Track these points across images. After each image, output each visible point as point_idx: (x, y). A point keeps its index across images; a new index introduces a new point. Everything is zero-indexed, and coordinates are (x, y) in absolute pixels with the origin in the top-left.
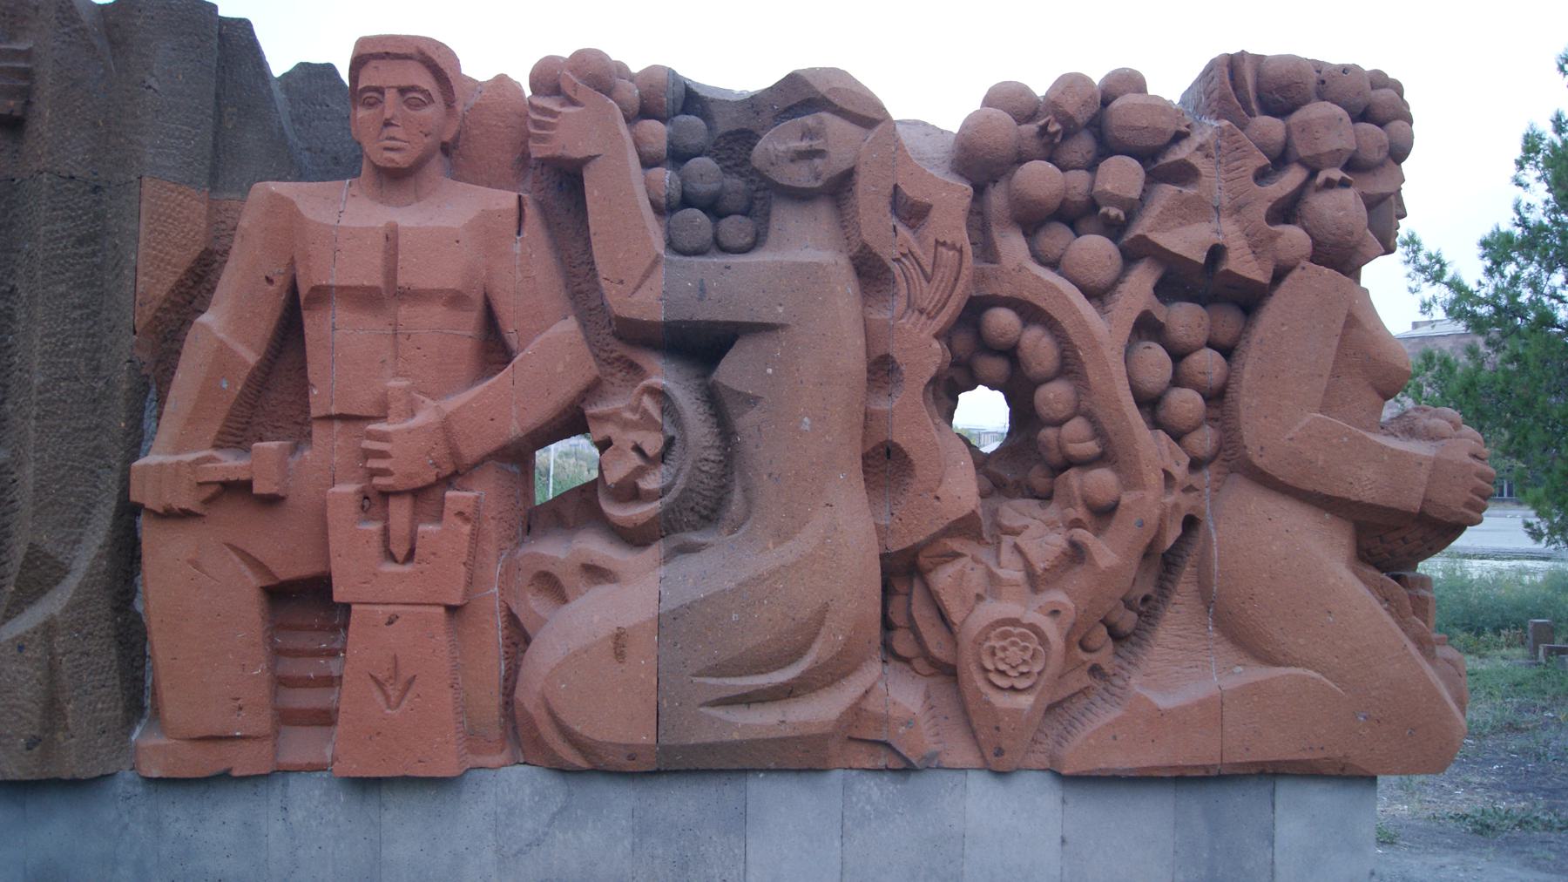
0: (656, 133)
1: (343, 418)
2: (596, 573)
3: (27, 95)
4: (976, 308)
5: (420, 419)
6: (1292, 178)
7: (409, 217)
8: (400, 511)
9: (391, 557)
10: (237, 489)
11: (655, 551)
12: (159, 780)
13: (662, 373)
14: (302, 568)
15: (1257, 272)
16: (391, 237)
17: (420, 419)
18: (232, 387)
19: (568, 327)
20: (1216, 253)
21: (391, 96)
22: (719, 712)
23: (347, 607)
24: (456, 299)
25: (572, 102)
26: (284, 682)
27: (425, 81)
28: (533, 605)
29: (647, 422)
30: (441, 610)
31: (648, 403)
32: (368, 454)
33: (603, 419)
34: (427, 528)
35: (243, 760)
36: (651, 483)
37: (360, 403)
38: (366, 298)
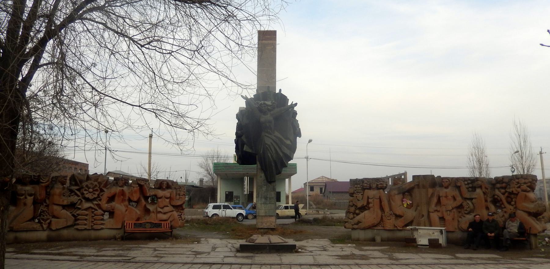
0: (466, 182)
4: (494, 196)
6: (519, 185)
10: (436, 211)
14: (441, 216)
15: (517, 193)
20: (512, 191)
36: (468, 210)
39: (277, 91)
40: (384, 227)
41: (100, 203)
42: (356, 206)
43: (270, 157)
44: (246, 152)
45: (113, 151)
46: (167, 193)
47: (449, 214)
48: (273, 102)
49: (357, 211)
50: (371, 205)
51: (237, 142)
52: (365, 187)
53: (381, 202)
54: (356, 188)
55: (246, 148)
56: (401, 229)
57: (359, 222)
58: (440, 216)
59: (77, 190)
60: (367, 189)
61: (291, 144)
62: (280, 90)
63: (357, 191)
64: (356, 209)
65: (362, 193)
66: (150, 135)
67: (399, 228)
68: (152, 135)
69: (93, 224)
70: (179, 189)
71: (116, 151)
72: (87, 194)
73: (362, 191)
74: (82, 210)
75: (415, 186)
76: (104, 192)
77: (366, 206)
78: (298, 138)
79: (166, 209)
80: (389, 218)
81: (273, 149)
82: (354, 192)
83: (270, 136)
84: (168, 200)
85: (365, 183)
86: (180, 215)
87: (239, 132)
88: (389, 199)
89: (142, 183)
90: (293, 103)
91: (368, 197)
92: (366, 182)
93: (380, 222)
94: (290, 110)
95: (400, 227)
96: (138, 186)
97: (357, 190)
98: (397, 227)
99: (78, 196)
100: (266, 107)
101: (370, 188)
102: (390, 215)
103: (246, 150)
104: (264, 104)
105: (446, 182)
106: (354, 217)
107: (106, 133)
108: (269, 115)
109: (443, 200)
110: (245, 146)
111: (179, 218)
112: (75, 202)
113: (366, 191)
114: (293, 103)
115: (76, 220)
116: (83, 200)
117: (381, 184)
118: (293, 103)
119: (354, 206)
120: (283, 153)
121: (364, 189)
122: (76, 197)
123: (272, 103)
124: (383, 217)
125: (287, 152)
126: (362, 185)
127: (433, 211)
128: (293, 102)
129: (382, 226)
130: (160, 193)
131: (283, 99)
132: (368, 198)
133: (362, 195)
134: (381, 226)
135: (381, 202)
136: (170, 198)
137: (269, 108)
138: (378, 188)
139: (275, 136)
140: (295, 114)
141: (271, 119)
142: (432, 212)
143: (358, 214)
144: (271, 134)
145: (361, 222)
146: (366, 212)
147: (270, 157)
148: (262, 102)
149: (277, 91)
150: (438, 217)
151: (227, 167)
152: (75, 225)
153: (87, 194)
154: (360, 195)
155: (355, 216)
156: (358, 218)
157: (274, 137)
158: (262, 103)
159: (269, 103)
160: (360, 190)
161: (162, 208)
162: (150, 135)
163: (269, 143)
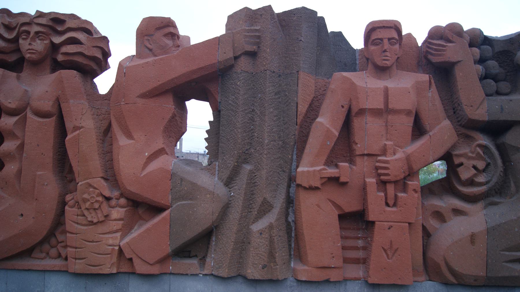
1: (368, 155)
2: (457, 212)
3: (258, 44)
5: (398, 156)
7: (390, 84)
9: (387, 205)
10: (334, 180)
11: (480, 205)
12: (305, 282)
13: (483, 140)
16: (386, 90)
17: (398, 156)
18: (330, 144)
19: (446, 123)
21: (386, 41)
22: (509, 265)
23: (373, 223)
24: (408, 113)
25: (450, 41)
26: (344, 248)
28: (433, 223)
29: (479, 157)
30: (407, 224)
31: (479, 150)
32: (377, 168)
33: (457, 156)
34: (400, 195)
35: (334, 276)
37: (375, 149)
38: (376, 113)
56: (155, 270)
58: (348, 209)
67: (140, 268)
75: (236, 58)
88: (110, 125)
98: (131, 260)
102: (100, 199)
124: (67, 208)
127: (318, 184)
142: (312, 189)
150: (336, 213)
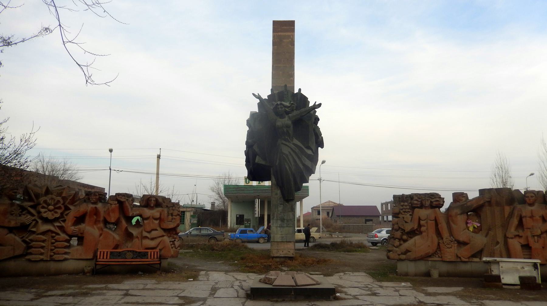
8: (536, 238)
14: (525, 243)
27: (533, 195)
39: (296, 91)
40: (441, 257)
41: (63, 224)
42: (404, 231)
43: (288, 170)
44: (259, 165)
45: (118, 171)
46: (156, 212)
47: (536, 241)
48: (292, 102)
49: (405, 237)
50: (423, 229)
51: (247, 153)
52: (414, 205)
53: (437, 224)
54: (402, 206)
55: (258, 160)
57: (407, 251)
58: (523, 243)
59: (31, 207)
60: (418, 207)
61: (313, 154)
62: (300, 90)
63: (404, 210)
64: (403, 234)
65: (411, 213)
66: (158, 155)
68: (160, 155)
69: (52, 254)
70: (172, 207)
71: (121, 171)
72: (45, 212)
73: (411, 211)
74: (38, 234)
75: (485, 203)
76: (69, 211)
77: (417, 229)
78: (319, 148)
79: (154, 234)
80: (449, 246)
81: (291, 160)
82: (400, 211)
83: (287, 144)
84: (157, 222)
85: (414, 199)
86: (173, 242)
87: (250, 141)
89: (123, 200)
90: (316, 104)
91: (419, 217)
92: (416, 198)
93: (436, 251)
94: (312, 112)
95: (465, 258)
96: (116, 202)
97: (403, 209)
98: (460, 258)
99: (33, 215)
100: (284, 109)
101: (422, 206)
103: (258, 162)
104: (281, 104)
105: (532, 197)
106: (400, 245)
107: (110, 152)
108: (287, 118)
109: (527, 222)
110: (257, 157)
111: (171, 245)
112: (28, 224)
113: (416, 210)
114: (316, 104)
115: (29, 247)
116: (40, 221)
117: (437, 201)
118: (317, 104)
119: (400, 230)
120: (304, 165)
121: (413, 208)
122: (29, 217)
123: (290, 103)
124: (440, 244)
125: (308, 163)
126: (410, 203)
127: (513, 237)
128: (316, 102)
129: (439, 257)
130: (147, 212)
131: (302, 99)
132: (420, 219)
133: (410, 215)
134: (437, 256)
135: (437, 224)
136: (160, 219)
137: (287, 109)
138: (432, 207)
139: (294, 144)
140: (317, 119)
141: (290, 122)
142: (512, 238)
143: (405, 241)
144: (289, 142)
145: (409, 251)
146: (417, 238)
147: (288, 170)
148: (279, 103)
149: (296, 91)
151: (238, 189)
152: (28, 254)
153: (45, 212)
154: (408, 215)
155: (402, 242)
156: (406, 245)
157: (293, 146)
158: (279, 104)
159: (287, 104)
160: (408, 209)
161: (149, 232)
162: (158, 155)
163: (287, 153)
